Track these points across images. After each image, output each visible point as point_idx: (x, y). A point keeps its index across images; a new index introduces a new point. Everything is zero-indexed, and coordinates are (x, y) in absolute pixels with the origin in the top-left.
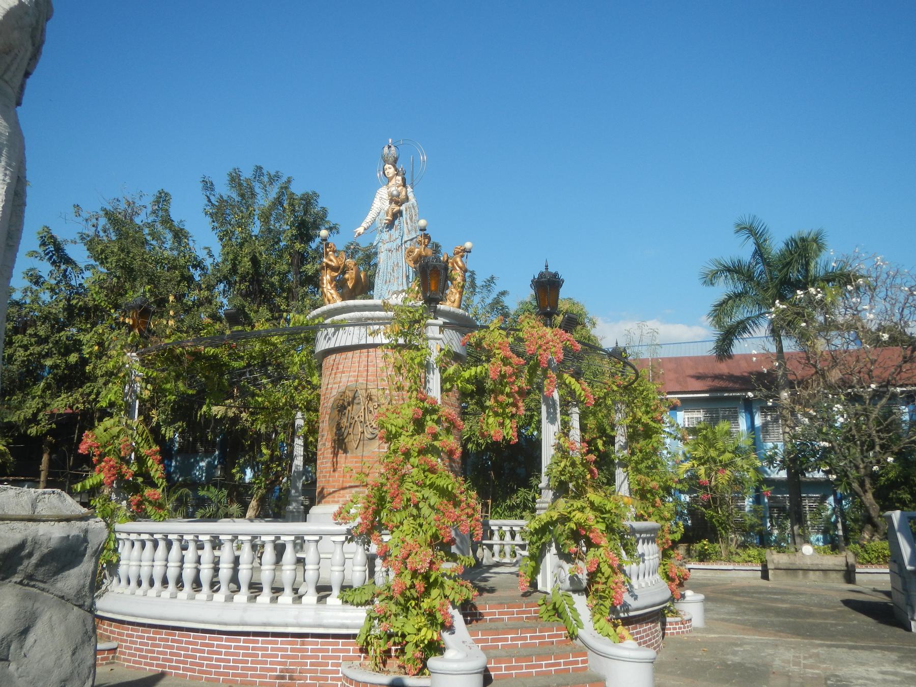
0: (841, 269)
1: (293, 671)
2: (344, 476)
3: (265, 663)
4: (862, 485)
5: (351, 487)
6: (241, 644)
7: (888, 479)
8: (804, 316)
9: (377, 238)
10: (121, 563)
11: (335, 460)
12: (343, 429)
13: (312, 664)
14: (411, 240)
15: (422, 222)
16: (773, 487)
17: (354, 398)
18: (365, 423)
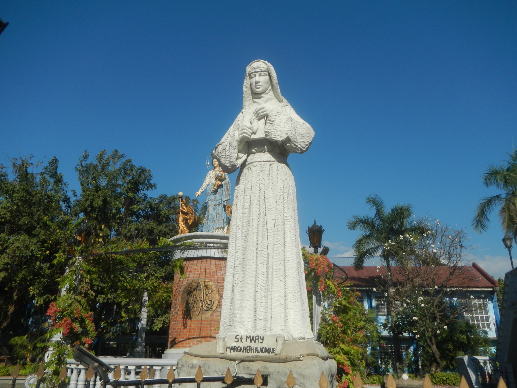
0: (419, 225)
2: (189, 332)
4: (431, 341)
5: (194, 338)
7: (442, 338)
8: (403, 249)
9: (208, 198)
10: (70, 383)
11: (185, 322)
12: (190, 305)
14: (227, 200)
16: (386, 341)
17: (197, 286)
18: (204, 301)
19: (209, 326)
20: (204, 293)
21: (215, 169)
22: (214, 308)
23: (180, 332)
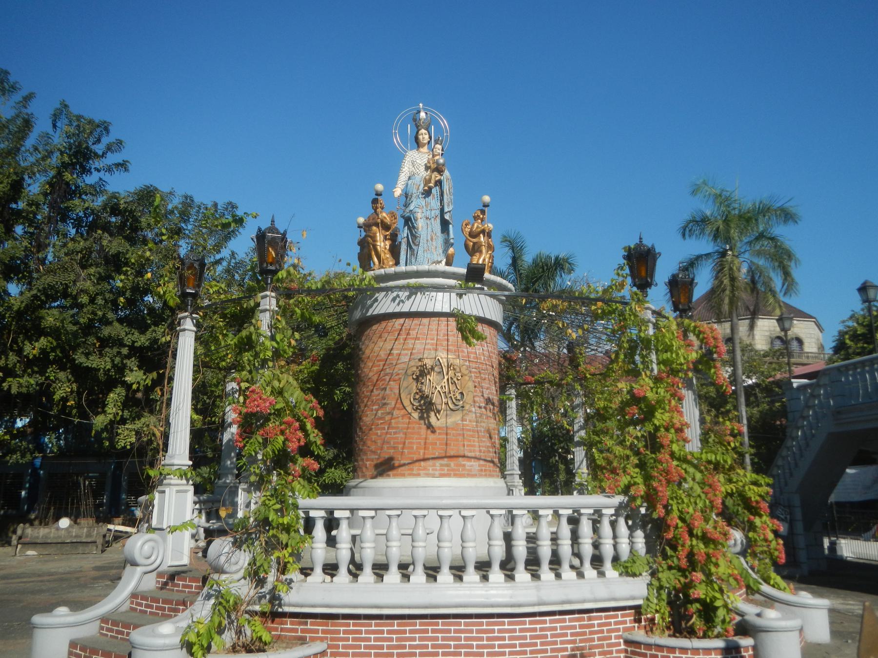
1: (582, 648)
3: (555, 643)
5: (433, 458)
6: (527, 626)
13: (599, 639)
14: (450, 212)
15: (487, 199)
19: (460, 438)
20: (448, 379)
21: (421, 150)
22: (467, 407)
23: (403, 448)
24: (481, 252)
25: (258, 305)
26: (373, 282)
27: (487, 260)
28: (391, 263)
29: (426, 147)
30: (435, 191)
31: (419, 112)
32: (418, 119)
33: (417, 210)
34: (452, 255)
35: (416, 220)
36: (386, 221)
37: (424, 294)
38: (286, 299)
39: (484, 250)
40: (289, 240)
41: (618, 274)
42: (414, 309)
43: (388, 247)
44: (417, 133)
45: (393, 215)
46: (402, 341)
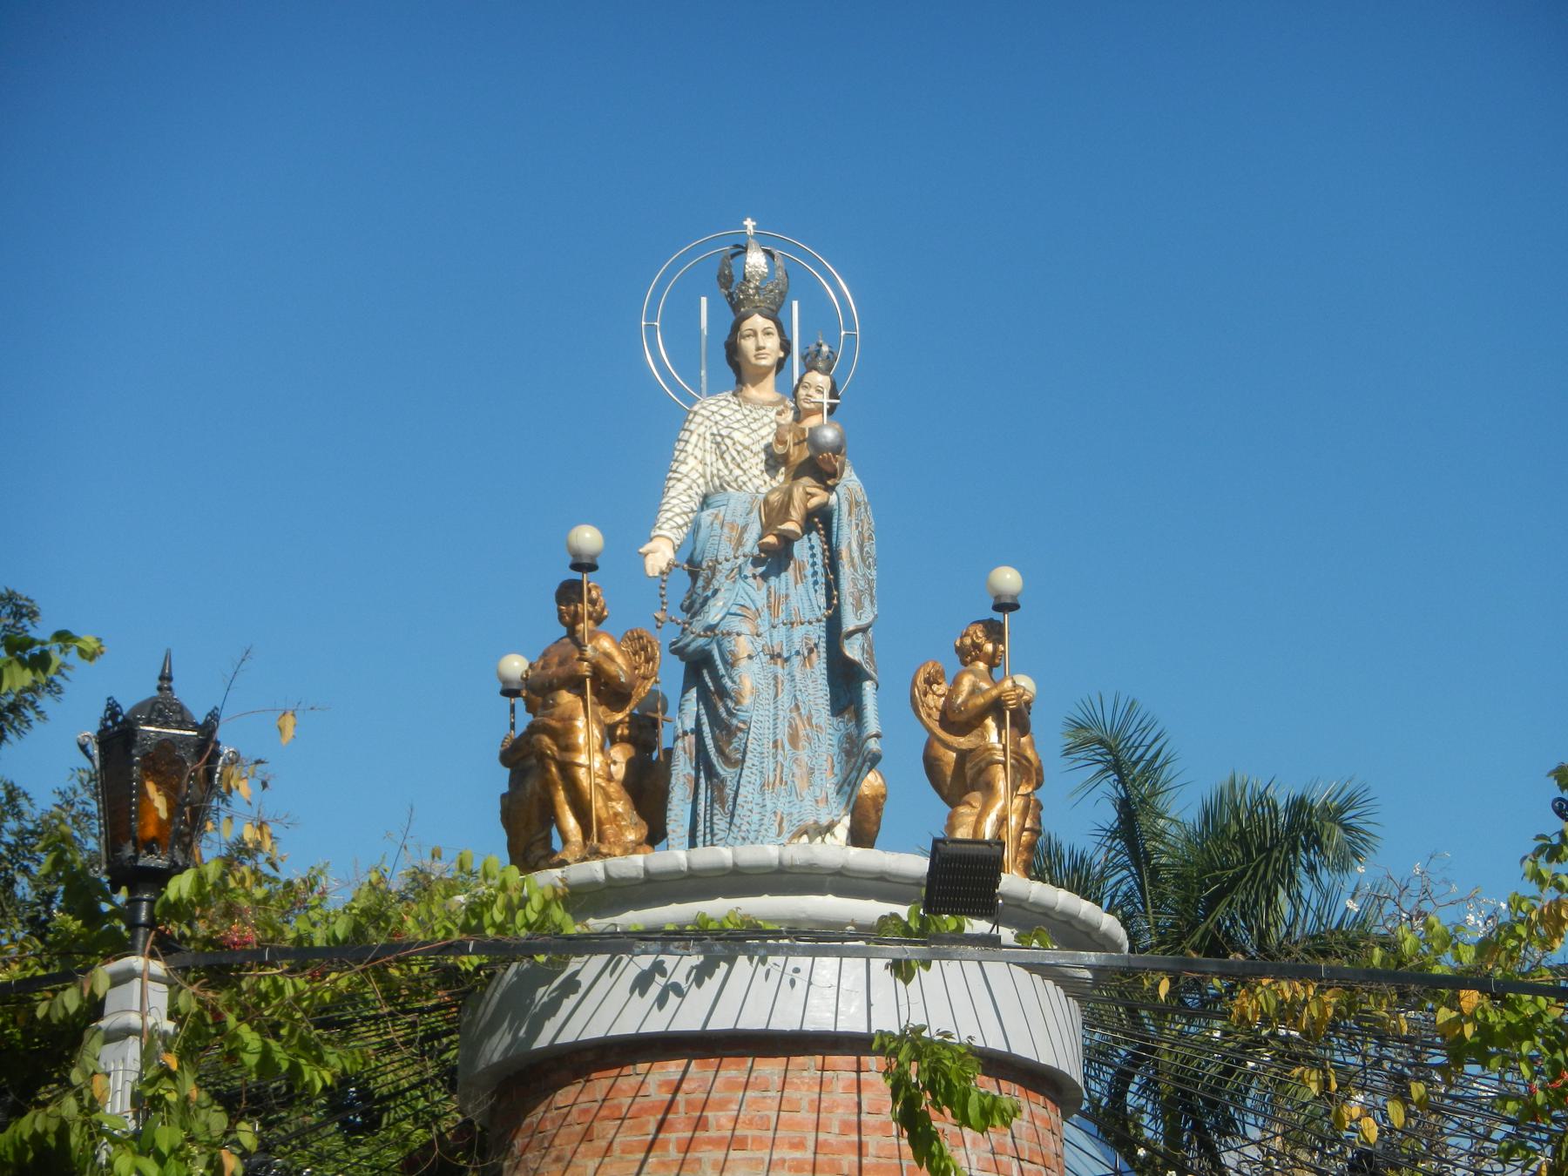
14: (863, 630)
15: (1008, 579)
21: (752, 392)
24: (989, 789)
25: (95, 1008)
26: (558, 914)
27: (1014, 820)
28: (631, 836)
29: (771, 380)
30: (807, 550)
31: (741, 250)
32: (738, 279)
33: (735, 624)
34: (878, 801)
35: (731, 664)
36: (611, 668)
37: (763, 961)
38: (206, 986)
39: (1001, 783)
40: (226, 750)
41: (1538, 877)
42: (722, 1022)
43: (619, 771)
44: (736, 328)
45: (639, 646)
46: (674, 1154)
